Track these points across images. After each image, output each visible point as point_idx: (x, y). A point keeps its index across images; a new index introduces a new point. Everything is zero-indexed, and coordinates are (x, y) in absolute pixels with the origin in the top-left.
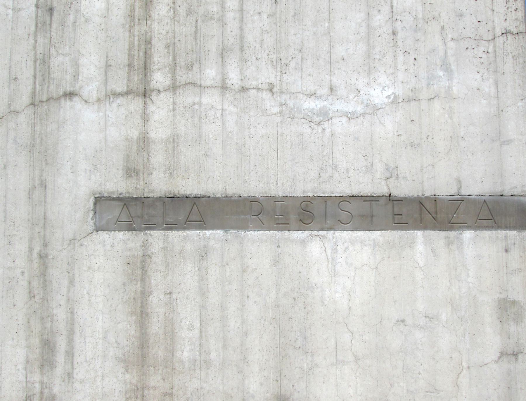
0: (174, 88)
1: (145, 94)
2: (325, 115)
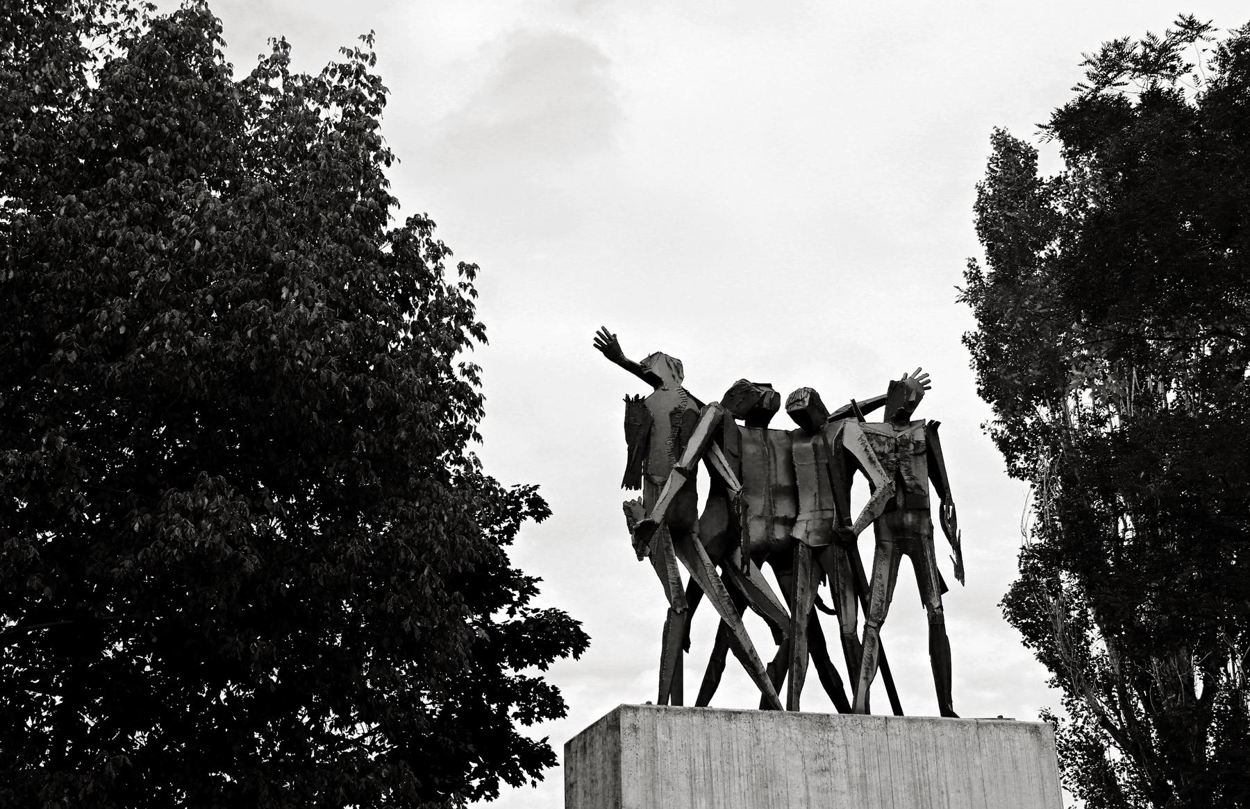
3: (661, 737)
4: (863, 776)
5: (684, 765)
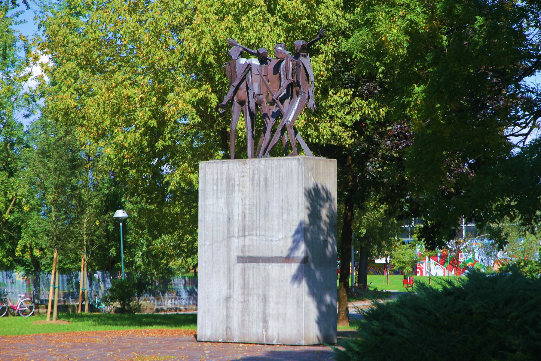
0: (249, 235)
1: (244, 236)
2: (272, 241)
3: (207, 170)
4: (253, 177)
5: (211, 177)
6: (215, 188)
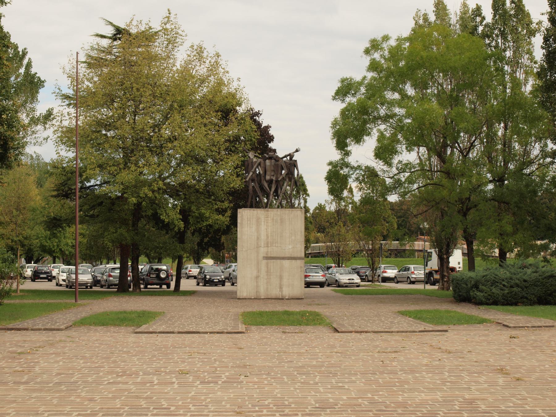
1: (268, 247)
2: (285, 249)
6: (249, 222)
